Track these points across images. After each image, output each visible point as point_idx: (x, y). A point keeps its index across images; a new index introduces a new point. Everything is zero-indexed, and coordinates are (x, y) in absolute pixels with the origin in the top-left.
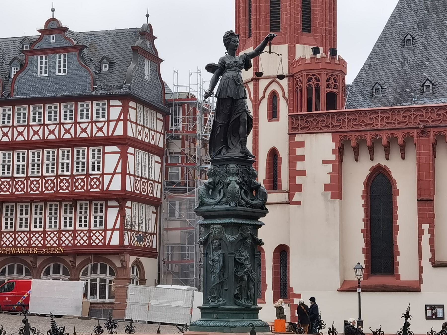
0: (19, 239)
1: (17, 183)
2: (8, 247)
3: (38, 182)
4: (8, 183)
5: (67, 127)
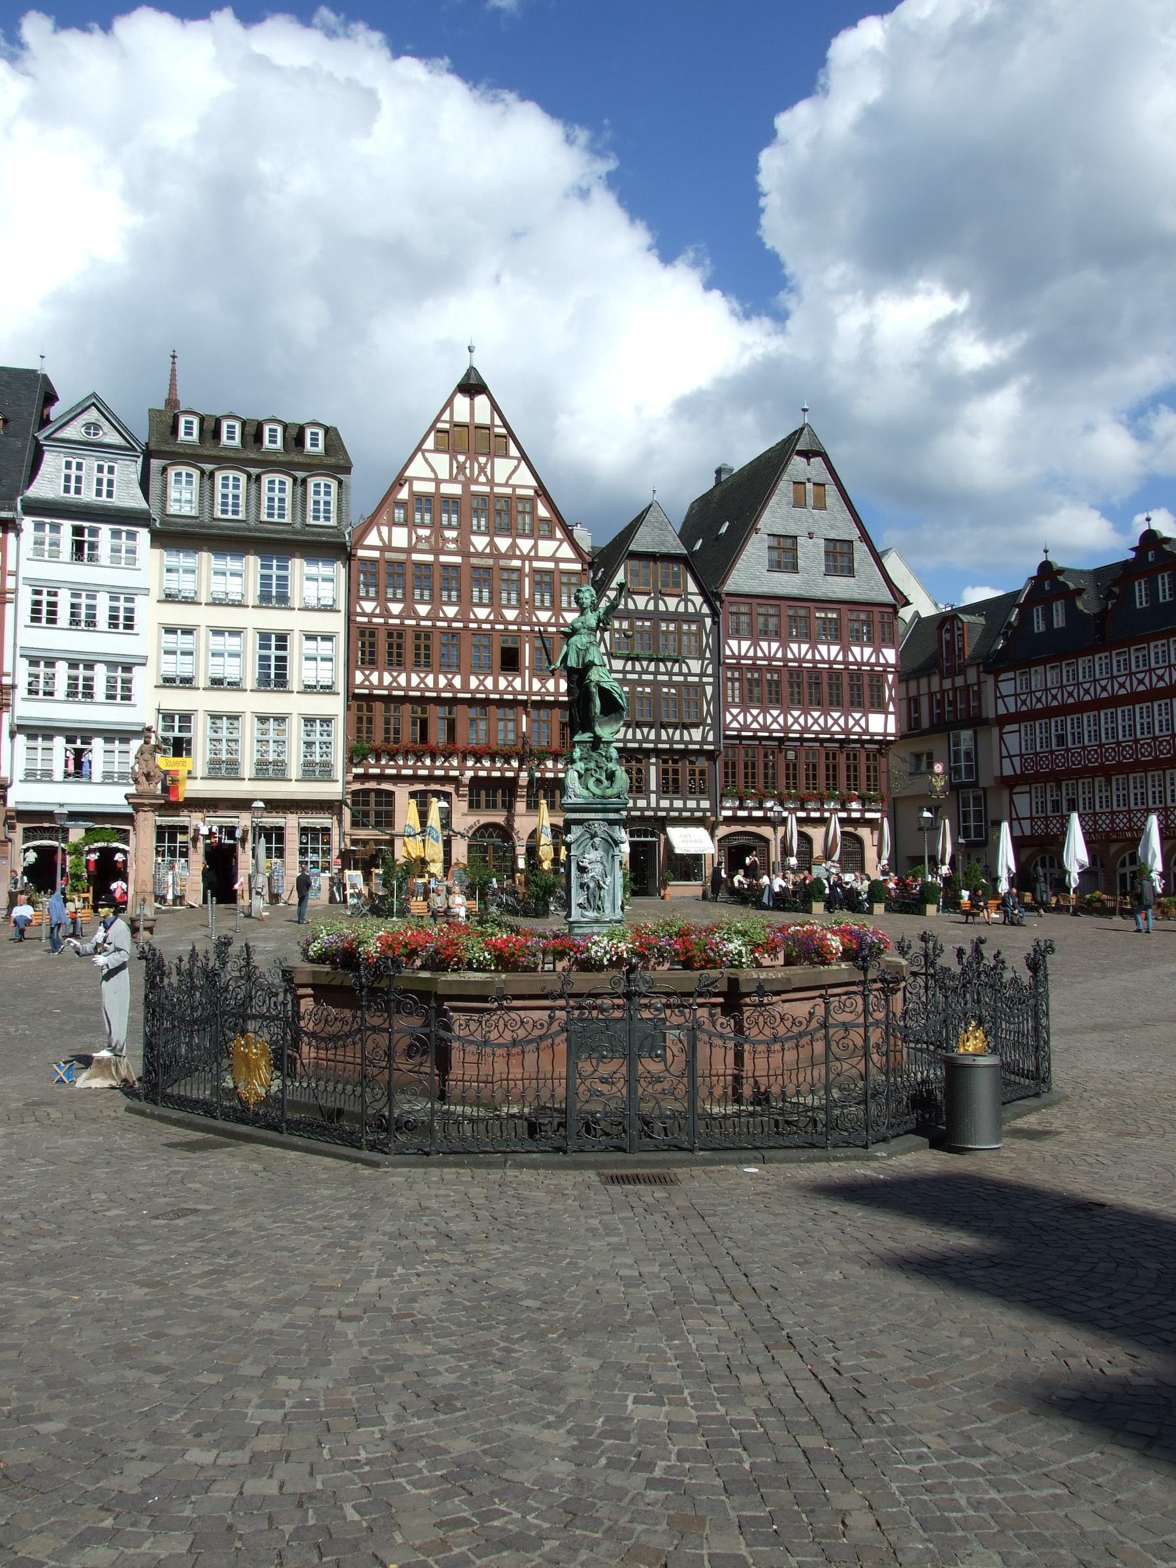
0: (1135, 820)
1: (1124, 748)
2: (1122, 830)
3: (1079, 754)
4: (1079, 754)
5: (1160, 672)
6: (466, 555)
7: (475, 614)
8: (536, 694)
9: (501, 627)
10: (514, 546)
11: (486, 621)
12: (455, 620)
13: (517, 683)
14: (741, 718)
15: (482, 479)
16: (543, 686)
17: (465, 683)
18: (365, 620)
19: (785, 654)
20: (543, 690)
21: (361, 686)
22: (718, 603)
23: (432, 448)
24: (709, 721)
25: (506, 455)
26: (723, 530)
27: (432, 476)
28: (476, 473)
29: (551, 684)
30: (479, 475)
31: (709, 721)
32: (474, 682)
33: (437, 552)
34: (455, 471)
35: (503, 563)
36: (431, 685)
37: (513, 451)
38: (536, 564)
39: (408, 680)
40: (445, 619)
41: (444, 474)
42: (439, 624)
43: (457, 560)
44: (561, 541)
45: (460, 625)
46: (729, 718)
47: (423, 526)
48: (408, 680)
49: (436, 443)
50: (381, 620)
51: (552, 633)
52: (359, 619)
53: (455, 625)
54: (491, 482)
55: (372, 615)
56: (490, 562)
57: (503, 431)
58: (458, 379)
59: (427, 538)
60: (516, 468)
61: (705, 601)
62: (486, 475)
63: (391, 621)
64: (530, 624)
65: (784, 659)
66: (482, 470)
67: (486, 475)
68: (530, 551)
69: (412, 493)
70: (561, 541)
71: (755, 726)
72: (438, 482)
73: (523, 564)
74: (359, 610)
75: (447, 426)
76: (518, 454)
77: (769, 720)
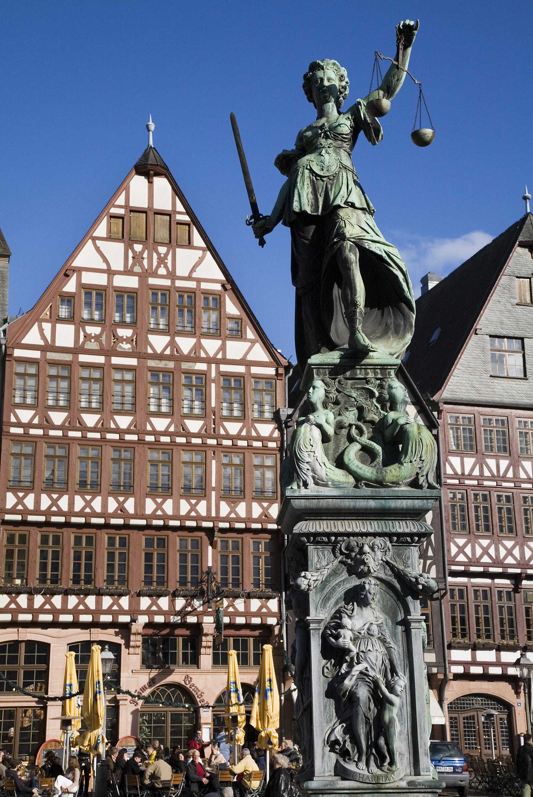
6: (142, 356)
7: (152, 425)
8: (224, 520)
9: (183, 440)
10: (198, 346)
11: (165, 433)
12: (128, 431)
13: (202, 508)
14: (468, 550)
15: (162, 271)
16: (233, 510)
17: (140, 505)
18: (20, 431)
19: (516, 473)
20: (233, 515)
21: (12, 511)
22: (435, 413)
23: (104, 235)
24: (430, 553)
25: (189, 245)
26: (435, 336)
27: (104, 267)
28: (155, 264)
29: (241, 509)
30: (158, 266)
31: (430, 553)
32: (150, 506)
33: (108, 353)
34: (131, 261)
35: (185, 366)
36: (98, 509)
37: (198, 240)
38: (224, 368)
39: (71, 503)
40: (117, 431)
41: (118, 265)
42: (109, 436)
43: (133, 362)
44: (253, 342)
45: (134, 437)
46: (454, 550)
47: (91, 322)
48: (71, 503)
49: (109, 230)
50: (40, 432)
51: (242, 448)
52: (13, 430)
53: (128, 437)
54: (172, 275)
55: (30, 425)
56: (171, 365)
57: (186, 218)
58: (136, 158)
59: (97, 338)
60: (201, 259)
61: (419, 412)
62: (166, 267)
63: (52, 433)
64: (218, 437)
65: (516, 479)
66: (162, 261)
67: (166, 267)
68: (217, 353)
69: (80, 286)
70: (253, 342)
71: (486, 559)
72: (110, 273)
73: (209, 368)
74: (13, 419)
75: (122, 211)
76: (204, 245)
77: (503, 552)
